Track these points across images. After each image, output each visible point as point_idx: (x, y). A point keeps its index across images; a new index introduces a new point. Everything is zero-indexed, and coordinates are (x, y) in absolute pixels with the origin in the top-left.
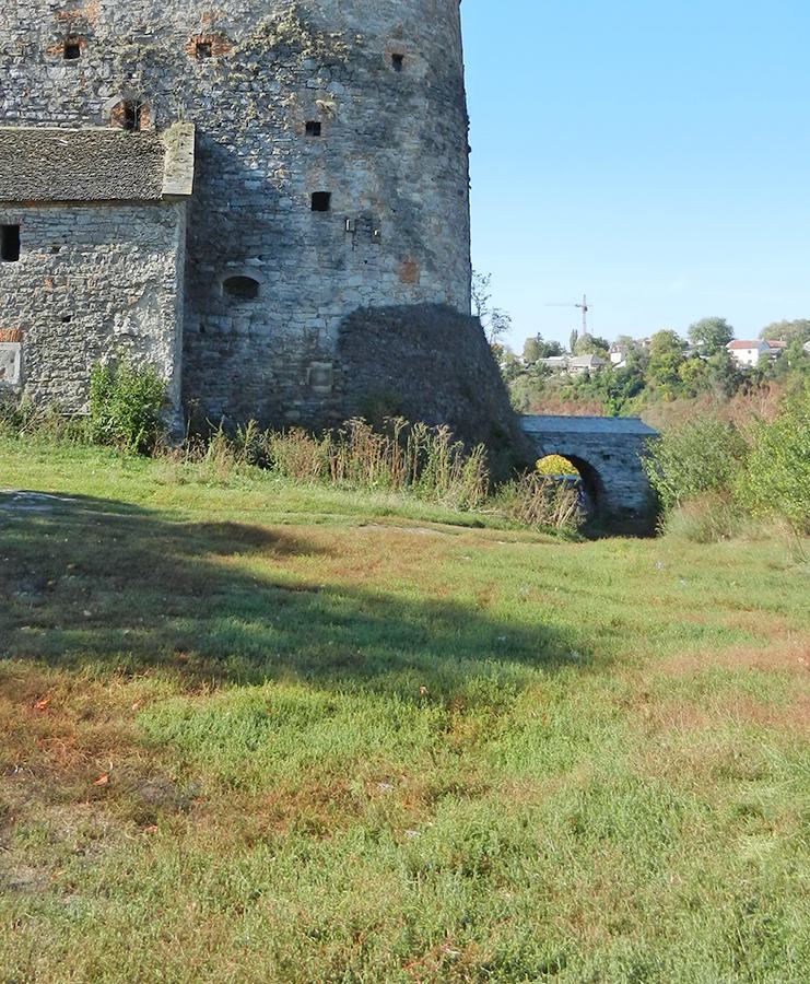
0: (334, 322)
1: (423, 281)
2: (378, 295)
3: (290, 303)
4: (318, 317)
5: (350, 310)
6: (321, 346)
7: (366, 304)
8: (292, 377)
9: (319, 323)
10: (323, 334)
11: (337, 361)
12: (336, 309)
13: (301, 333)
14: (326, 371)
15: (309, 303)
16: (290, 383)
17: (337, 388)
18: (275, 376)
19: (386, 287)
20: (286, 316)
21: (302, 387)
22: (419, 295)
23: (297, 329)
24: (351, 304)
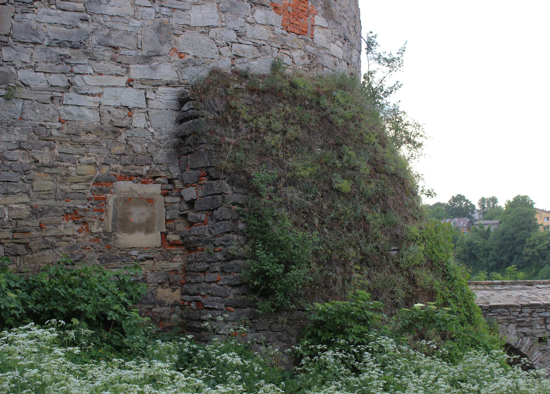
0: (165, 98)
1: (319, 36)
2: (247, 49)
3: (67, 51)
4: (130, 83)
5: (196, 74)
6: (138, 148)
7: (224, 65)
8: (73, 215)
9: (131, 97)
10: (139, 121)
11: (170, 181)
12: (166, 71)
13: (92, 117)
14: (150, 201)
15: (109, 54)
16: (69, 228)
17: (172, 237)
18: (36, 212)
19: (260, 33)
20: (59, 80)
21: (97, 237)
22: (313, 59)
23: (83, 111)
24: (195, 62)
